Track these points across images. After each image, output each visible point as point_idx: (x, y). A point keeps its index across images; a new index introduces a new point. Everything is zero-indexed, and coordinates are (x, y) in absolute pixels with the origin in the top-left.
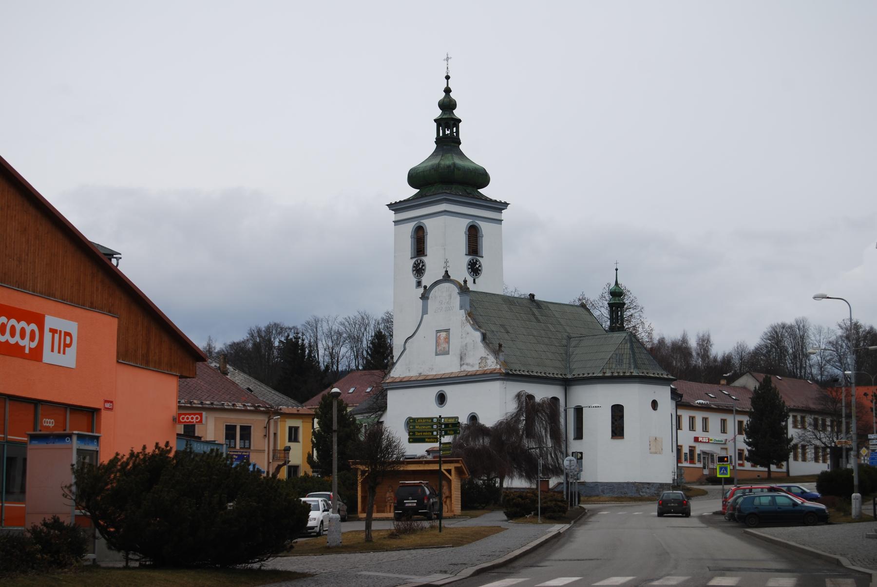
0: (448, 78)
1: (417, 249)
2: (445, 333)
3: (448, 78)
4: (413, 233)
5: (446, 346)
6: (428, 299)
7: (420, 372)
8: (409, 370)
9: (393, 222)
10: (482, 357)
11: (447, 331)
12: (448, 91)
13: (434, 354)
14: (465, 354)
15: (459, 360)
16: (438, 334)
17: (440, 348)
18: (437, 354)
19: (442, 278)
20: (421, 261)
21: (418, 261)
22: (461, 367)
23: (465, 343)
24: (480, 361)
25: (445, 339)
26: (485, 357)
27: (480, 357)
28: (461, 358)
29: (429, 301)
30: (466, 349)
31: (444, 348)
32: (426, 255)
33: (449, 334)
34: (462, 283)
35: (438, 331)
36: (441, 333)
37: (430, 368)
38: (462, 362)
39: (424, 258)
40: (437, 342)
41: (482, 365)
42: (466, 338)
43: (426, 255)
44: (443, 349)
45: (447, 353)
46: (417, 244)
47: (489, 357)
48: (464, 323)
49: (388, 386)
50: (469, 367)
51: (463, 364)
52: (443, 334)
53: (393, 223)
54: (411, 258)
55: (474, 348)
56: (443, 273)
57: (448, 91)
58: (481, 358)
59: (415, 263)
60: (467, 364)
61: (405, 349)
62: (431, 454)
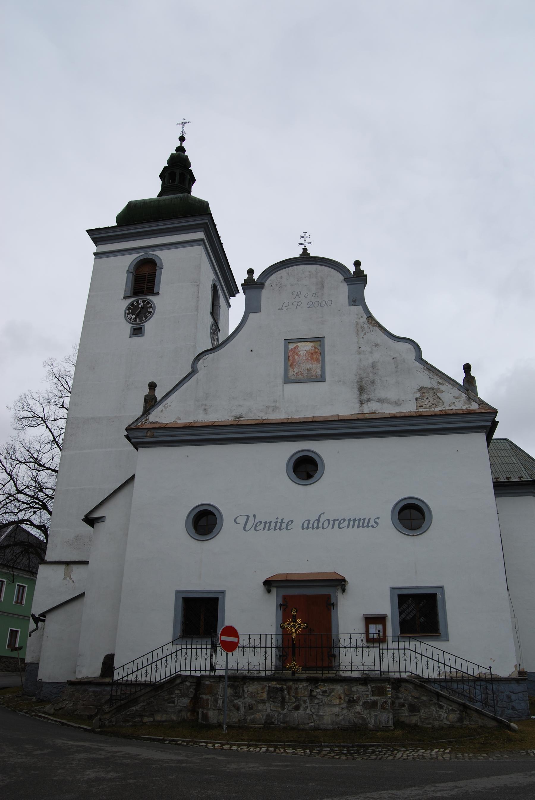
0: (182, 139)
1: (134, 290)
2: (311, 344)
3: (182, 139)
4: (132, 268)
5: (316, 367)
6: (263, 289)
7: (238, 414)
8: (205, 410)
9: (94, 254)
10: (423, 387)
11: (319, 341)
12: (181, 149)
13: (280, 380)
14: (373, 382)
15: (356, 392)
16: (291, 346)
17: (296, 370)
18: (287, 381)
19: (299, 256)
20: (144, 301)
21: (138, 302)
22: (364, 403)
23: (371, 361)
24: (418, 395)
25: (312, 354)
26: (432, 389)
27: (416, 387)
28: (361, 390)
29: (264, 292)
30: (373, 373)
31: (309, 370)
32: (158, 294)
33: (322, 346)
34: (352, 269)
35: (288, 341)
36: (299, 344)
37: (268, 407)
38: (365, 397)
39: (152, 298)
40: (287, 358)
41: (427, 402)
42: (371, 352)
43: (158, 294)
44: (305, 372)
45: (322, 379)
46: (135, 284)
47: (442, 387)
48: (362, 328)
49: (146, 437)
50: (385, 405)
51: (368, 400)
52: (308, 346)
53: (94, 256)
54: (125, 298)
55: (397, 372)
56: (301, 252)
57: (181, 149)
58: (419, 390)
59: (132, 304)
60: (380, 400)
61: (194, 371)
62: (274, 591)
